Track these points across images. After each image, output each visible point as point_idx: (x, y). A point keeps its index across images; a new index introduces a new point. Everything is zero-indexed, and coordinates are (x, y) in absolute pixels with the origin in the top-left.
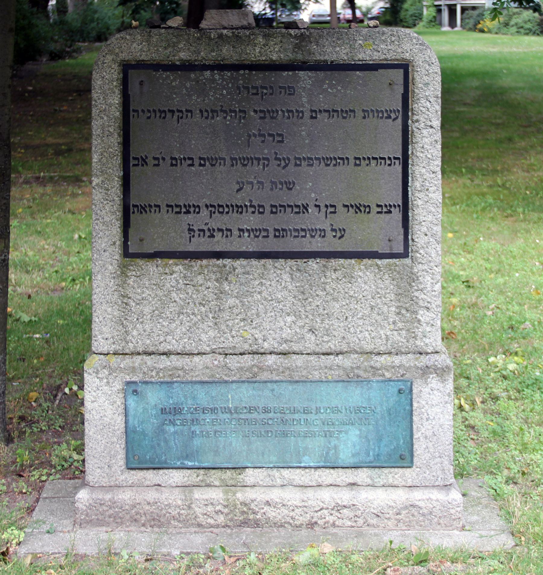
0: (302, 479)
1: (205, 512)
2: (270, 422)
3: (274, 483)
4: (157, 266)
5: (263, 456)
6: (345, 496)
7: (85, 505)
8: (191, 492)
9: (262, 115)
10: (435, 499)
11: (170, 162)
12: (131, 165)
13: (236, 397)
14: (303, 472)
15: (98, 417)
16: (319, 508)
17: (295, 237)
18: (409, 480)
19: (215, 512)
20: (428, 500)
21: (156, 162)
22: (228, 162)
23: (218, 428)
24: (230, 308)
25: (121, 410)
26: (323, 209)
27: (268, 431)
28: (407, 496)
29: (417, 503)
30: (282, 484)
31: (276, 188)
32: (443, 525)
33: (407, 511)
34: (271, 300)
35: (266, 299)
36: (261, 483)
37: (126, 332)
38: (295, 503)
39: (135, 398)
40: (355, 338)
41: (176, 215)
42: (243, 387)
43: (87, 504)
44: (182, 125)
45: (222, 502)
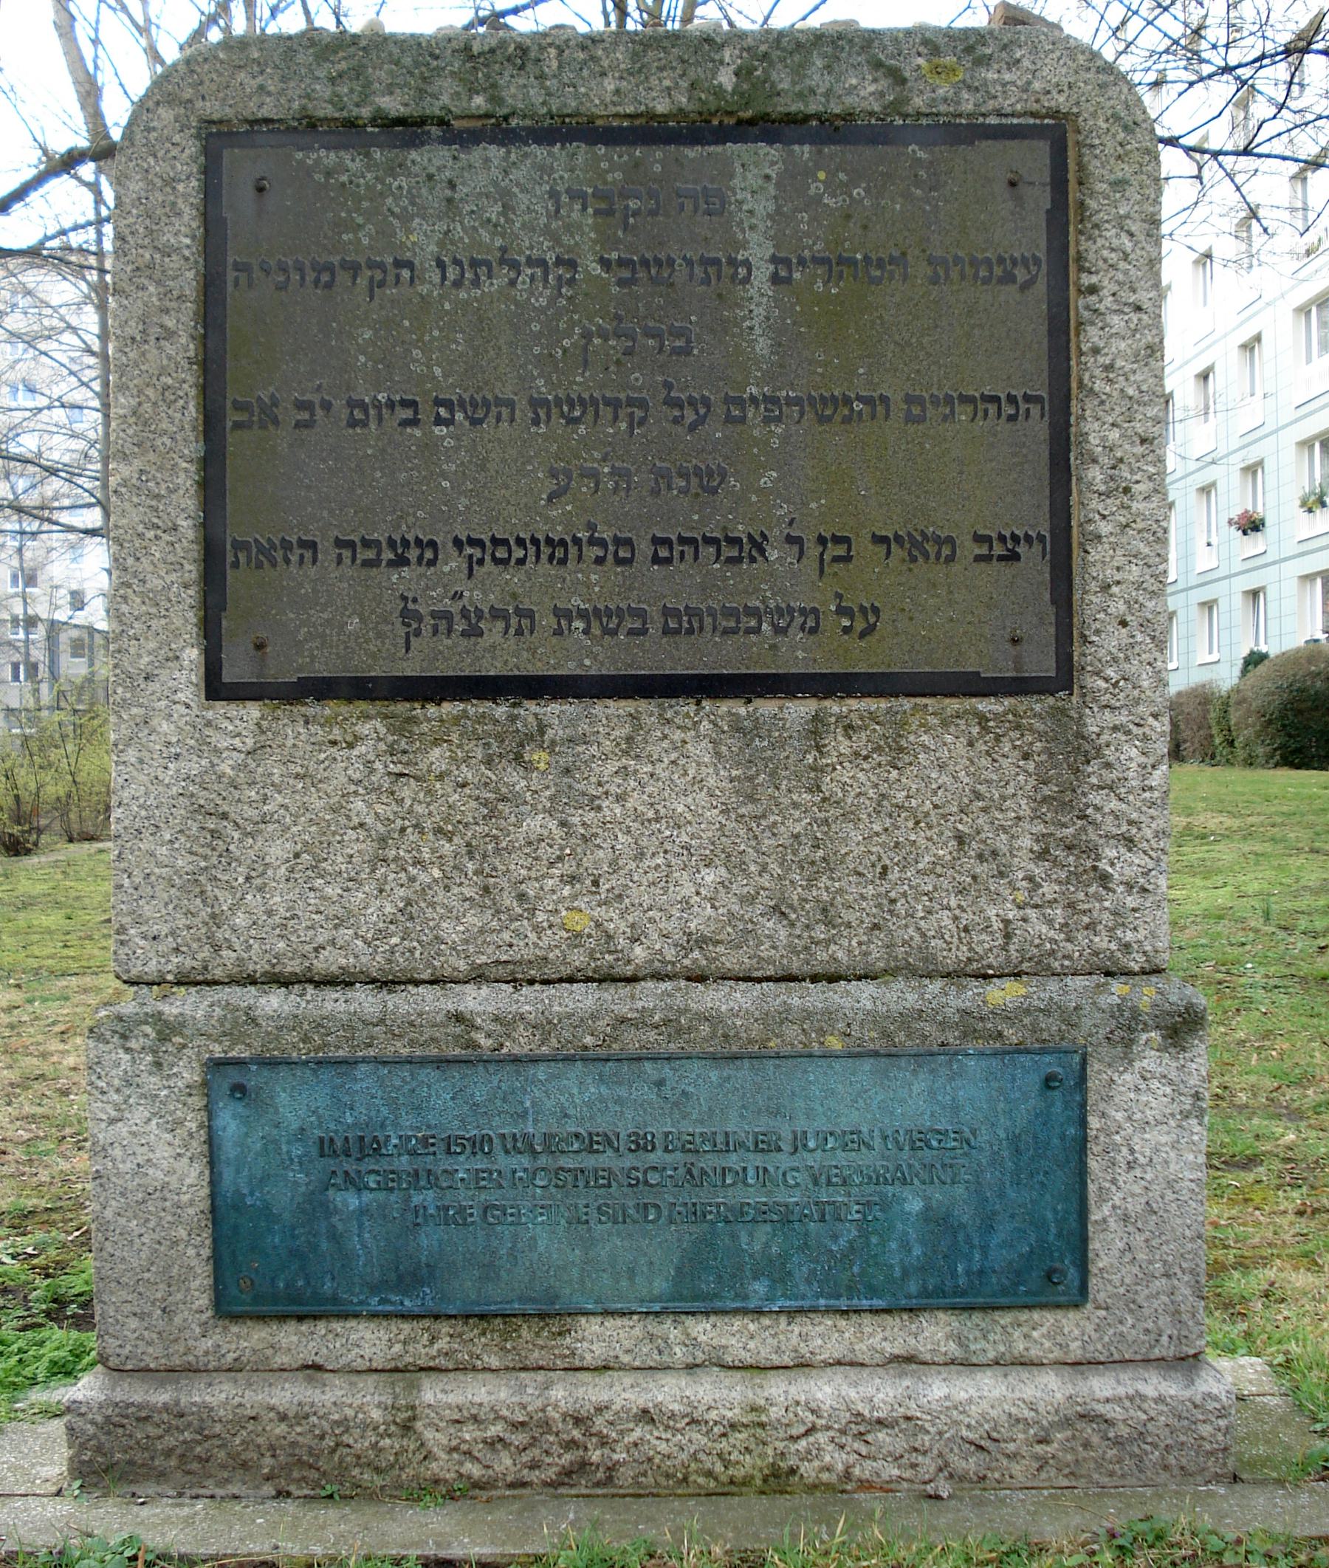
0: (752, 1345)
1: (454, 1443)
2: (653, 1178)
3: (665, 1358)
4: (307, 722)
5: (631, 1279)
6: (881, 1393)
7: (93, 1423)
8: (414, 1387)
9: (626, 274)
10: (1156, 1394)
11: (345, 414)
12: (229, 424)
13: (549, 1104)
14: (752, 1327)
15: (127, 1167)
16: (802, 1430)
17: (726, 632)
18: (1075, 1345)
19: (484, 1442)
20: (1131, 1398)
21: (305, 416)
22: (523, 411)
23: (492, 1197)
24: (530, 843)
25: (197, 1146)
26: (813, 550)
27: (646, 1205)
28: (1070, 1390)
29: (1101, 1409)
30: (690, 1360)
31: (669, 488)
32: (1176, 1471)
33: (1069, 1433)
34: (657, 820)
35: (638, 816)
36: (626, 1359)
37: (213, 916)
38: (729, 1414)
39: (240, 1108)
40: (911, 931)
41: (364, 572)
42: (572, 1075)
43: (99, 1419)
44: (382, 307)
45: (505, 1413)
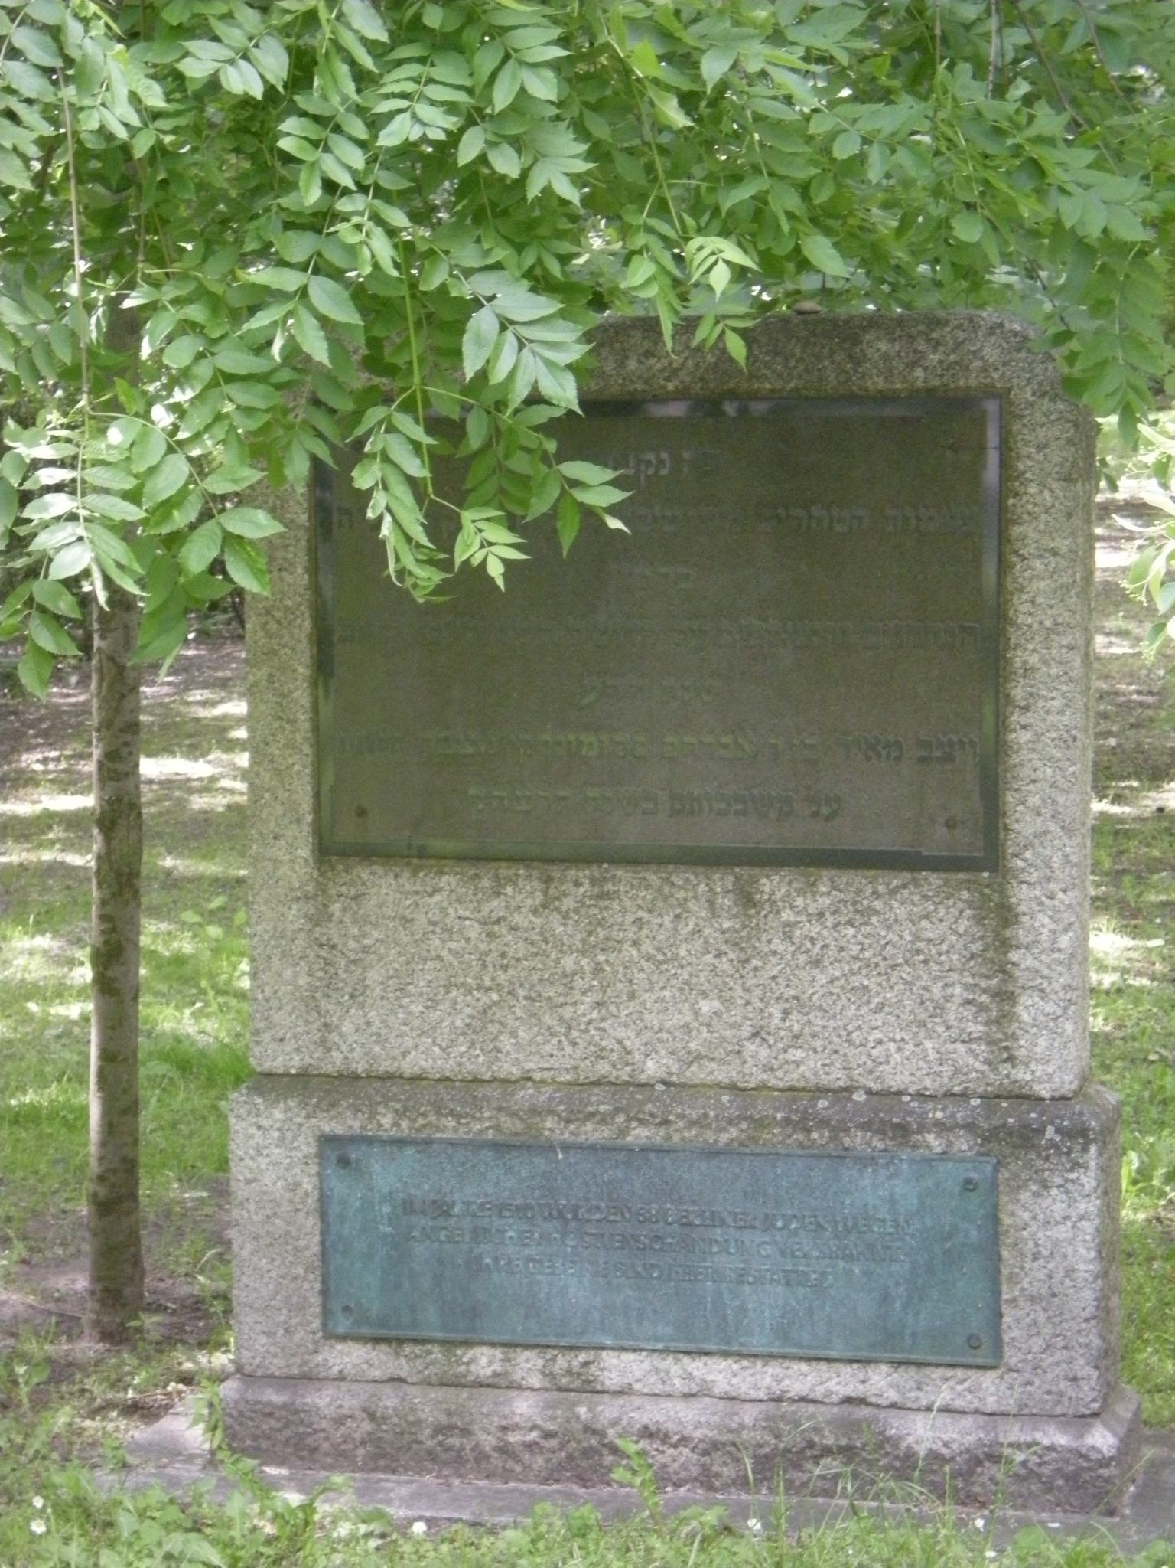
0: (734, 1381)
14: (735, 1367)
18: (991, 1399)
40: (864, 1058)
